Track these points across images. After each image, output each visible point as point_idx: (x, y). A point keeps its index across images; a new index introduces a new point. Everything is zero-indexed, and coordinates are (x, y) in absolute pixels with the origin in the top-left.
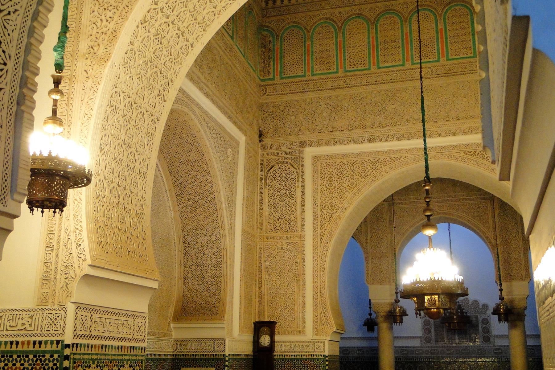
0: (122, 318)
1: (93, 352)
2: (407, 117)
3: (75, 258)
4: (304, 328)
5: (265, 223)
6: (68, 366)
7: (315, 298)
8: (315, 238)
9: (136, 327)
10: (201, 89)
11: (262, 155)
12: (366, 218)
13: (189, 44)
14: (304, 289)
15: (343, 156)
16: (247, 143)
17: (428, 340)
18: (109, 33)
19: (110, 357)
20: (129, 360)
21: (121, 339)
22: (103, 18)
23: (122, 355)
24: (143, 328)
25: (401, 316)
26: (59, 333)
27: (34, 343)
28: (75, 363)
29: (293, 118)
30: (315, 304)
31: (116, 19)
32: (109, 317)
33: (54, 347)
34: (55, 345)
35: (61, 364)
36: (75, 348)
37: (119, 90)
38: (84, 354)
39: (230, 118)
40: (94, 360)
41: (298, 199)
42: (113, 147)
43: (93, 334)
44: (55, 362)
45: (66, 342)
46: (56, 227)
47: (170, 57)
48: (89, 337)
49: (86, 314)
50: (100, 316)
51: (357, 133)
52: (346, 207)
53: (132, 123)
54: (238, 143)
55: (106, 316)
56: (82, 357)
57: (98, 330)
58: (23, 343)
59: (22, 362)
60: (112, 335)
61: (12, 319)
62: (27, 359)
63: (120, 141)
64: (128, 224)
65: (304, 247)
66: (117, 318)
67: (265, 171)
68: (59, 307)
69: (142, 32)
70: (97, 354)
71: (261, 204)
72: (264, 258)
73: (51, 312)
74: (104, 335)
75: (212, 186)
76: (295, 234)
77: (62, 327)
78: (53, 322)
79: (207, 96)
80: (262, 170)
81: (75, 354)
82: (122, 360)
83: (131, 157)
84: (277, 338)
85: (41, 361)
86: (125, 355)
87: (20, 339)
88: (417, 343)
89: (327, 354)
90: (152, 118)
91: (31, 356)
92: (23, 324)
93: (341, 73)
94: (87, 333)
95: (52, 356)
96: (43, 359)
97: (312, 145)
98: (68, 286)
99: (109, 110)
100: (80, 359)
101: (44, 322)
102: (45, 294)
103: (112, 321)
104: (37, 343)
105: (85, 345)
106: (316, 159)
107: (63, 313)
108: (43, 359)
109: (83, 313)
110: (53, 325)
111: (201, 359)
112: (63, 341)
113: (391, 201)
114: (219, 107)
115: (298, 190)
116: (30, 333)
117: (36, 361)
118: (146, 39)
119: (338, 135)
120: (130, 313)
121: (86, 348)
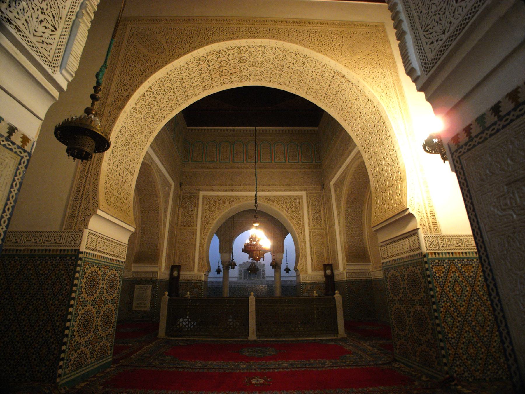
0: (114, 244)
1: (96, 259)
2: (243, 183)
3: (91, 205)
4: (194, 269)
5: (179, 223)
6: (80, 264)
7: (199, 256)
8: (201, 230)
9: (121, 251)
10: (158, 157)
11: (181, 193)
12: (221, 226)
13: (163, 116)
14: (195, 252)
15: (216, 196)
16: (175, 186)
17: (241, 278)
18: (125, 96)
19: (105, 263)
20: (115, 267)
21: (112, 255)
22: (122, 89)
23: (112, 264)
24: (124, 252)
25: (234, 266)
26: (77, 245)
27: (61, 250)
28: (85, 262)
29: (196, 178)
30: (199, 259)
31: (129, 90)
32: (106, 242)
33: (73, 253)
34: (73, 252)
35: (77, 262)
36: (86, 254)
37: (126, 126)
38: (91, 259)
39: (169, 173)
40: (96, 263)
41: (195, 213)
42: (119, 154)
43: (97, 249)
44: (73, 261)
45: (81, 250)
46: (82, 188)
47: (153, 119)
48: (95, 250)
49: (94, 237)
50: (102, 240)
51: (222, 187)
52: (216, 218)
53: (130, 146)
54: (171, 186)
55: (105, 241)
56: (89, 260)
57: (100, 247)
58: (53, 250)
59: (52, 261)
60: (107, 251)
61: (48, 237)
62: (55, 259)
63: (123, 152)
64: (122, 196)
65: (196, 234)
66: (111, 243)
67: (181, 201)
68: (78, 231)
69: (142, 102)
70: (98, 260)
71: (178, 214)
72: (178, 237)
73: (73, 233)
74: (103, 251)
75: (158, 202)
76: (193, 228)
77: (79, 242)
78: (74, 239)
79: (160, 161)
80: (180, 199)
81: (85, 258)
82: (111, 266)
83: (127, 163)
84: (181, 273)
85: (64, 260)
86: (114, 264)
87: (52, 248)
88: (236, 280)
89: (203, 280)
90: (140, 147)
91: (58, 258)
92: (55, 240)
93: (218, 162)
94: (94, 248)
95: (71, 258)
96: (65, 259)
97: (203, 191)
98: (85, 220)
99: (119, 134)
100: (88, 261)
101: (68, 239)
102: (70, 224)
103: (108, 245)
104: (63, 250)
105: (92, 254)
106: (204, 197)
107: (81, 234)
108: (65, 259)
109: (92, 236)
110: (74, 241)
111: (146, 281)
112: (79, 250)
113: (238, 214)
114: (165, 167)
115: (195, 209)
116: (58, 245)
117: (61, 260)
118: (143, 105)
119: (215, 187)
120: (119, 242)
121: (92, 256)
